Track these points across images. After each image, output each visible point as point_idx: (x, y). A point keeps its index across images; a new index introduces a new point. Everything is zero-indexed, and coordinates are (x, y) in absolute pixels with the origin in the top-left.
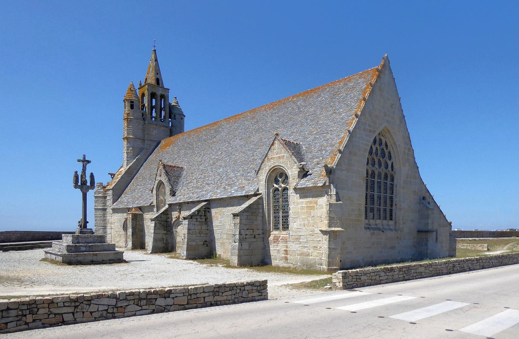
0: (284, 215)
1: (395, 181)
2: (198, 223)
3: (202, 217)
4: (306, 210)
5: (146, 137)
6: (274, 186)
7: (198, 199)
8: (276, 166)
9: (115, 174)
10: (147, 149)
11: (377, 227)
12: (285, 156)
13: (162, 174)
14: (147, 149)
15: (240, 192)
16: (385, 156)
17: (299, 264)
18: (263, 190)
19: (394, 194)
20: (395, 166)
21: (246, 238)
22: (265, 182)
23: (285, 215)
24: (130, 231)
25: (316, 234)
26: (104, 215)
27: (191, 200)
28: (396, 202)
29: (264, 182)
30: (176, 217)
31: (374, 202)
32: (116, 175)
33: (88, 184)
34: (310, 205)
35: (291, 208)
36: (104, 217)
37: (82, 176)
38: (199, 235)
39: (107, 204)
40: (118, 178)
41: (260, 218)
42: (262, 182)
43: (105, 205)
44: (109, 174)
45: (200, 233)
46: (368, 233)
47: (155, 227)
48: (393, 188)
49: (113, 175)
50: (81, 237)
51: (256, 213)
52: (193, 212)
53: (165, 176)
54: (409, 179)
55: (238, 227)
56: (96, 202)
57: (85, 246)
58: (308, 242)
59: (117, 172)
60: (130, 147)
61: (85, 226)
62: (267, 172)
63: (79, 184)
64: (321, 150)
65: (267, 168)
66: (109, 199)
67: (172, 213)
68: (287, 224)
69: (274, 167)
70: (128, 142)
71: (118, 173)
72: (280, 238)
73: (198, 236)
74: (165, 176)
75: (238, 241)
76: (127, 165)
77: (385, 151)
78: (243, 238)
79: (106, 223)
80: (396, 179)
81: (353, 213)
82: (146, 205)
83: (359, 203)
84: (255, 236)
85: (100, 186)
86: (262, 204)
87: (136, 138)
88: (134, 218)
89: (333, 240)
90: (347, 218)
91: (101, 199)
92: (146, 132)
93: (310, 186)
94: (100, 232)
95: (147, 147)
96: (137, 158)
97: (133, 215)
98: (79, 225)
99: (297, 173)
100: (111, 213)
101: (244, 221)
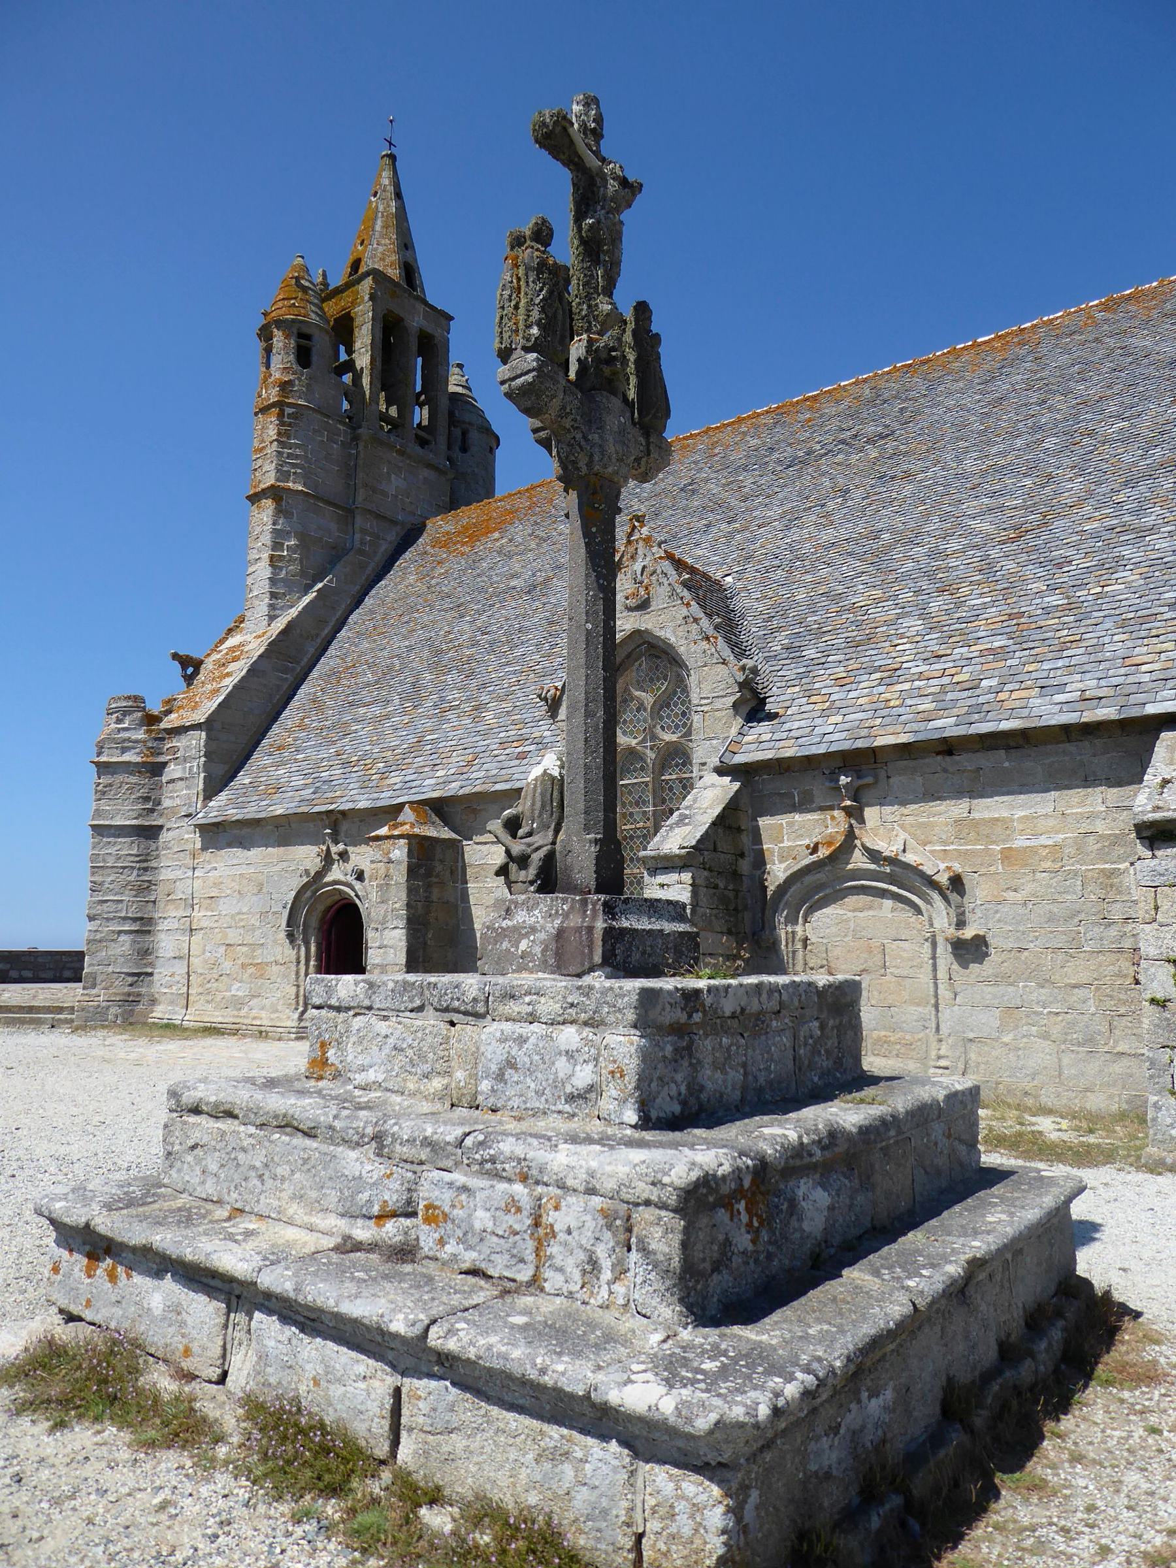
5: (360, 498)
9: (201, 662)
10: (361, 552)
14: (361, 552)
26: (145, 864)
30: (815, 850)
32: (209, 665)
39: (167, 803)
40: (228, 675)
43: (152, 811)
44: (175, 656)
53: (688, 605)
56: (101, 794)
59: (213, 650)
60: (288, 533)
66: (181, 779)
67: (764, 822)
70: (279, 512)
71: (215, 656)
74: (688, 605)
76: (272, 618)
79: (154, 902)
82: (498, 787)
85: (130, 713)
87: (315, 498)
88: (419, 866)
91: (133, 779)
92: (361, 475)
94: (118, 951)
95: (362, 542)
96: (320, 585)
97: (414, 842)
100: (190, 846)
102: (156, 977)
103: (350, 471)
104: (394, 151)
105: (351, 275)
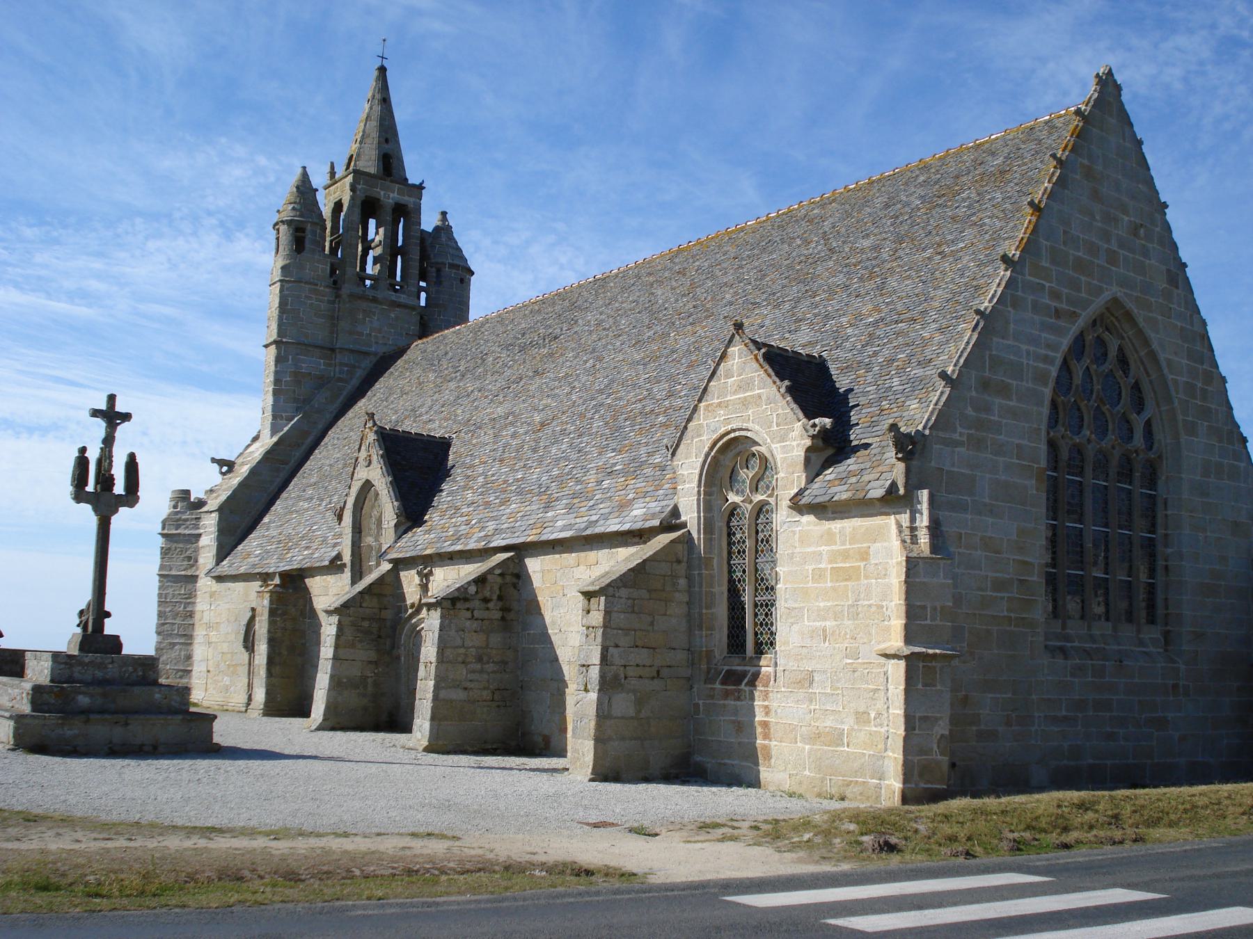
0: (759, 598)
1: (1161, 483)
2: (475, 625)
3: (491, 605)
4: (831, 581)
6: (728, 500)
7: (483, 543)
8: (734, 431)
11: (1094, 646)
12: (764, 398)
13: (374, 458)
15: (617, 520)
16: (1120, 399)
17: (807, 773)
18: (690, 515)
19: (1160, 531)
20: (1158, 435)
21: (626, 678)
22: (699, 486)
23: (764, 598)
24: (262, 648)
25: (865, 666)
27: (458, 548)
28: (1166, 561)
29: (695, 484)
31: (1082, 557)
34: (844, 565)
35: (781, 573)
36: (189, 603)
37: (99, 462)
38: (478, 666)
41: (677, 610)
42: (687, 486)
43: (192, 566)
44: (214, 460)
45: (480, 659)
47: (338, 637)
48: (1154, 511)
49: (227, 466)
50: (81, 664)
51: (664, 590)
52: (459, 588)
55: (599, 639)
58: (838, 694)
61: (99, 626)
62: (706, 449)
63: (90, 488)
64: (888, 377)
65: (704, 438)
68: (769, 629)
69: (728, 433)
72: (746, 680)
73: (473, 672)
75: (598, 688)
77: (1119, 383)
78: (616, 677)
80: (1163, 478)
81: (1002, 595)
83: (1027, 559)
84: (658, 672)
86: (685, 559)
88: (277, 609)
89: (920, 686)
90: (977, 612)
93: (844, 496)
97: (274, 595)
98: (81, 622)
99: (803, 454)
101: (620, 619)
102: (194, 673)
103: (333, 319)
104: (386, 63)
105: (346, 170)
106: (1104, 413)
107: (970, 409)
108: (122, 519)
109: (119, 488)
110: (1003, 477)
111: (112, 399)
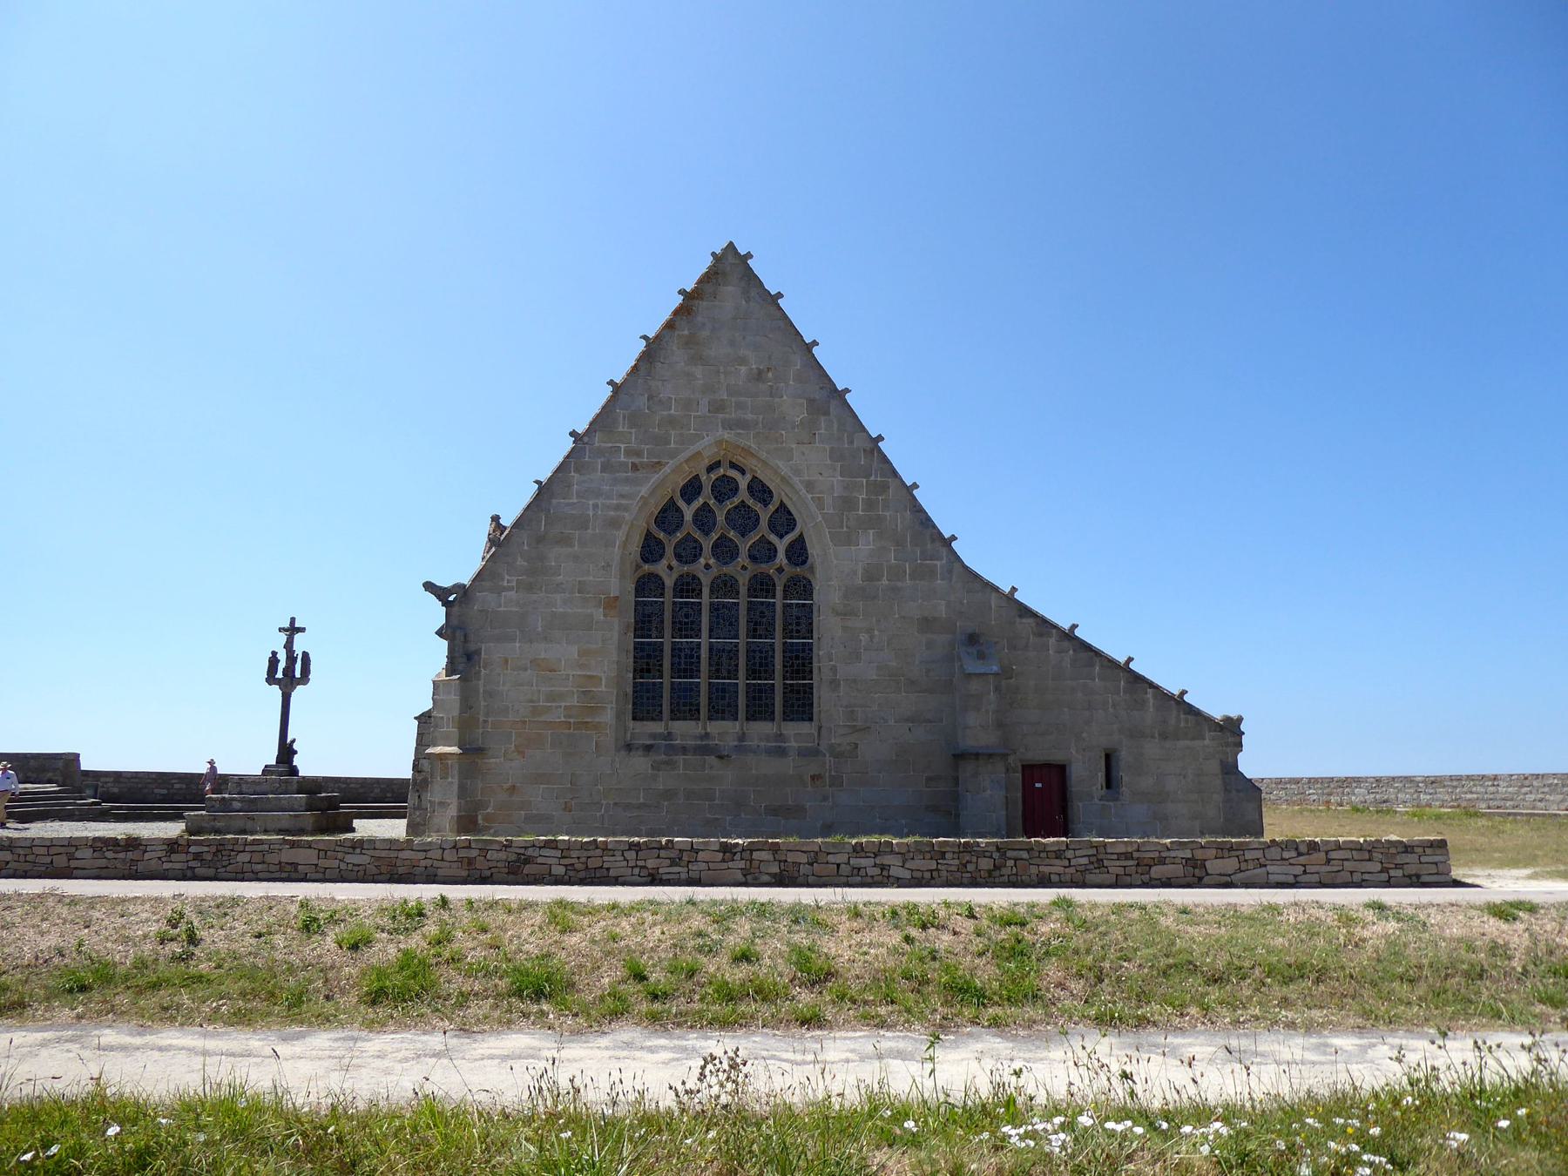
33: (298, 674)
46: (640, 763)
54: (885, 582)
57: (241, 801)
90: (572, 720)
106: (731, 540)
107: (519, 559)
108: (299, 693)
109: (298, 674)
110: (561, 610)
111: (293, 620)
